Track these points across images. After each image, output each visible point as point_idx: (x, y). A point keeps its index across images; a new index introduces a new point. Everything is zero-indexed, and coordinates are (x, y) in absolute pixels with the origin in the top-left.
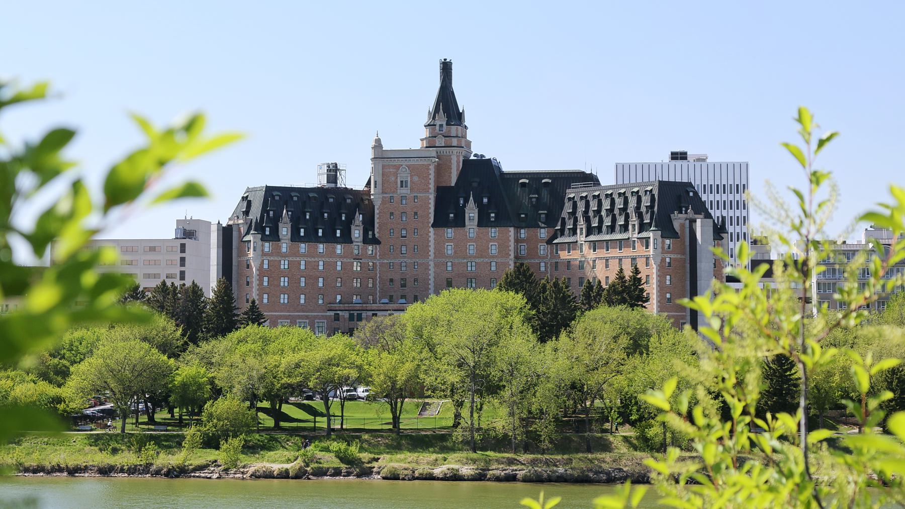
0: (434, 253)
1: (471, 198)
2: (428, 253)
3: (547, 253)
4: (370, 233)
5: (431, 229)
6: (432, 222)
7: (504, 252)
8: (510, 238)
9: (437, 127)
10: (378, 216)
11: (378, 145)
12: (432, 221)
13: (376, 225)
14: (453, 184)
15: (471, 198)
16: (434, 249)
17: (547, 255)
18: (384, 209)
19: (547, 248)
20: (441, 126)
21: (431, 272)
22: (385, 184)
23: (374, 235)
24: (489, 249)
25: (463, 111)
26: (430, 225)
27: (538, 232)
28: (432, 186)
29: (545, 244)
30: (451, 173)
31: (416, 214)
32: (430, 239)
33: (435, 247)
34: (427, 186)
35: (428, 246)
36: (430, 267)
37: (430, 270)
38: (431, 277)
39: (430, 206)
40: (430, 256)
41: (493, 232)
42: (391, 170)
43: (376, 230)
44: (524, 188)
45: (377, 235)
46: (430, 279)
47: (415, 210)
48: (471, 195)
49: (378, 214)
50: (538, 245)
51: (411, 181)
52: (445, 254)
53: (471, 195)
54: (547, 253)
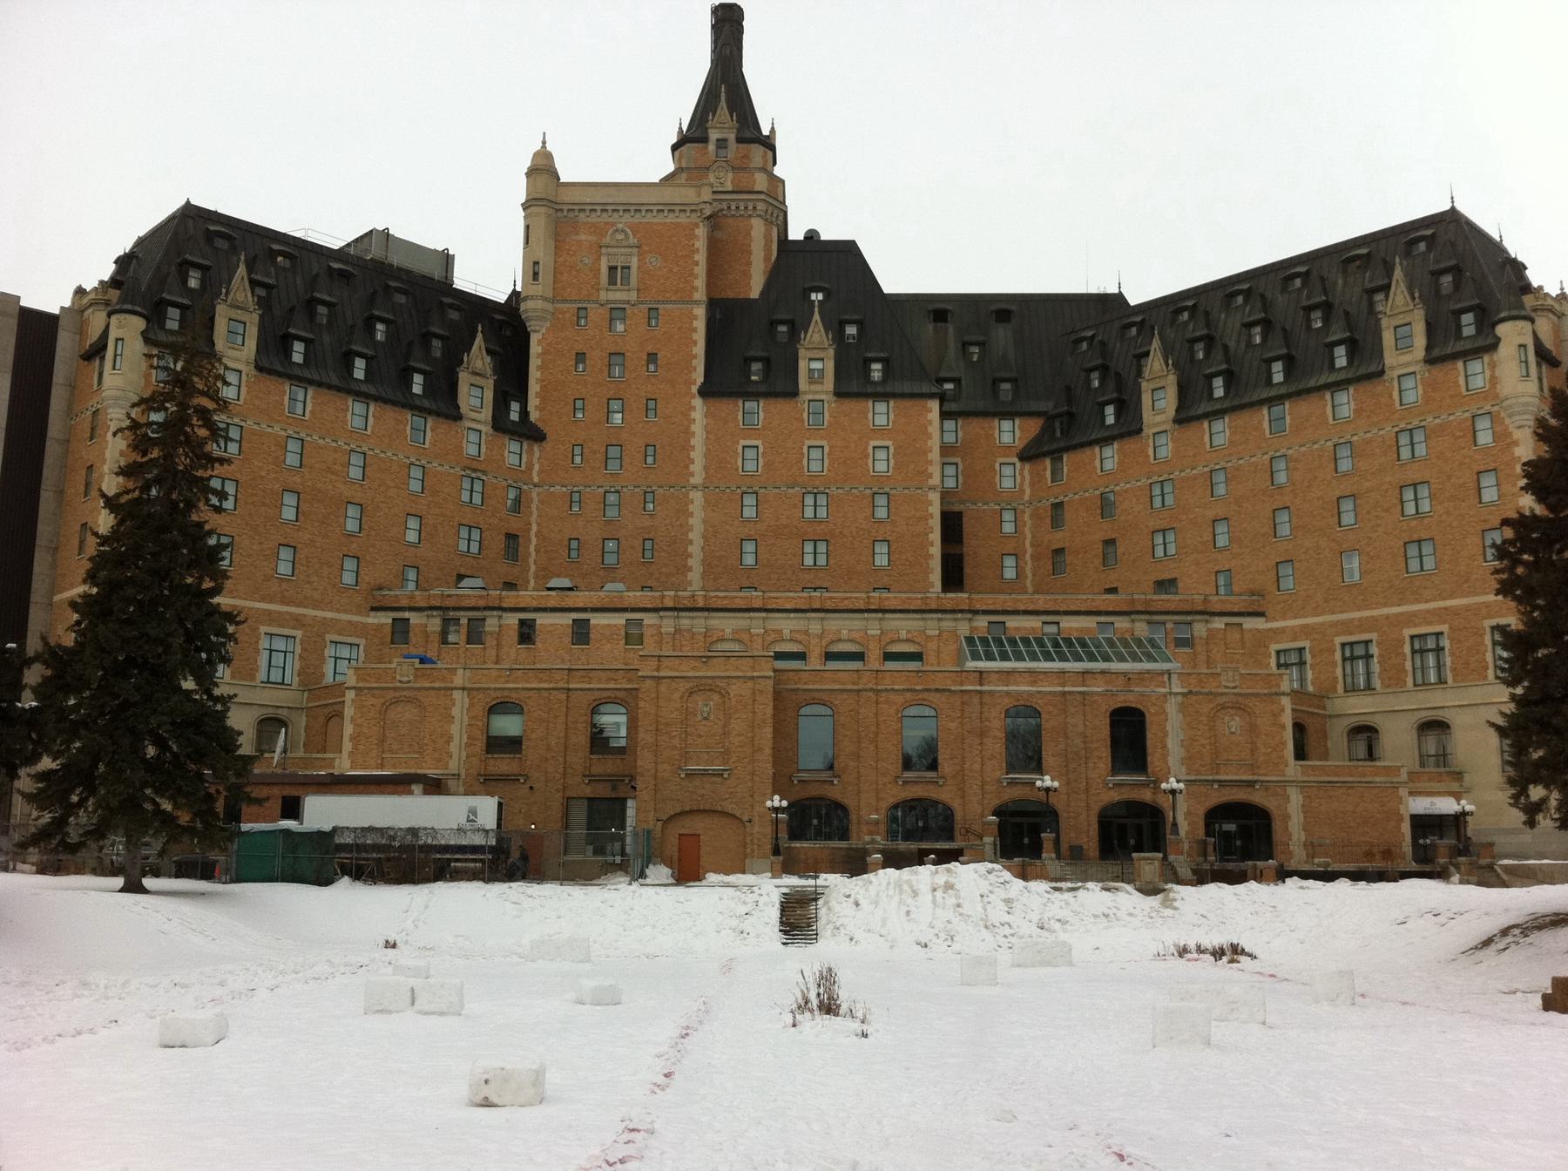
0: (706, 468)
1: (817, 317)
2: (687, 467)
3: (1022, 484)
4: (515, 407)
5: (698, 402)
6: (700, 379)
7: (912, 467)
8: (930, 429)
9: (711, 147)
10: (539, 362)
11: (542, 168)
12: (699, 377)
13: (534, 387)
14: (755, 293)
15: (817, 317)
16: (706, 456)
17: (1022, 491)
18: (558, 343)
19: (1022, 470)
20: (722, 143)
21: (696, 522)
22: (562, 273)
23: (524, 413)
24: (867, 456)
25: (773, 130)
26: (694, 389)
27: (992, 428)
28: (700, 294)
29: (1015, 460)
30: (749, 264)
31: (652, 357)
32: (693, 428)
33: (708, 449)
34: (687, 282)
35: (687, 448)
36: (691, 508)
37: (691, 515)
38: (696, 536)
39: (695, 336)
40: (692, 474)
41: (881, 413)
42: (583, 237)
43: (533, 402)
44: (939, 324)
45: (534, 416)
46: (691, 542)
47: (650, 348)
48: (816, 309)
49: (539, 355)
50: (995, 462)
51: (639, 267)
52: (737, 469)
53: (816, 309)
54: (1022, 484)
